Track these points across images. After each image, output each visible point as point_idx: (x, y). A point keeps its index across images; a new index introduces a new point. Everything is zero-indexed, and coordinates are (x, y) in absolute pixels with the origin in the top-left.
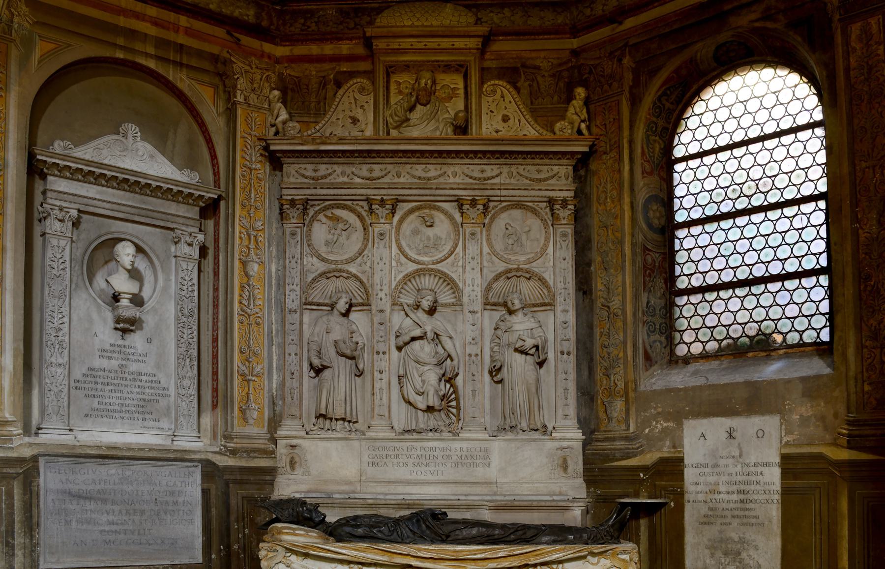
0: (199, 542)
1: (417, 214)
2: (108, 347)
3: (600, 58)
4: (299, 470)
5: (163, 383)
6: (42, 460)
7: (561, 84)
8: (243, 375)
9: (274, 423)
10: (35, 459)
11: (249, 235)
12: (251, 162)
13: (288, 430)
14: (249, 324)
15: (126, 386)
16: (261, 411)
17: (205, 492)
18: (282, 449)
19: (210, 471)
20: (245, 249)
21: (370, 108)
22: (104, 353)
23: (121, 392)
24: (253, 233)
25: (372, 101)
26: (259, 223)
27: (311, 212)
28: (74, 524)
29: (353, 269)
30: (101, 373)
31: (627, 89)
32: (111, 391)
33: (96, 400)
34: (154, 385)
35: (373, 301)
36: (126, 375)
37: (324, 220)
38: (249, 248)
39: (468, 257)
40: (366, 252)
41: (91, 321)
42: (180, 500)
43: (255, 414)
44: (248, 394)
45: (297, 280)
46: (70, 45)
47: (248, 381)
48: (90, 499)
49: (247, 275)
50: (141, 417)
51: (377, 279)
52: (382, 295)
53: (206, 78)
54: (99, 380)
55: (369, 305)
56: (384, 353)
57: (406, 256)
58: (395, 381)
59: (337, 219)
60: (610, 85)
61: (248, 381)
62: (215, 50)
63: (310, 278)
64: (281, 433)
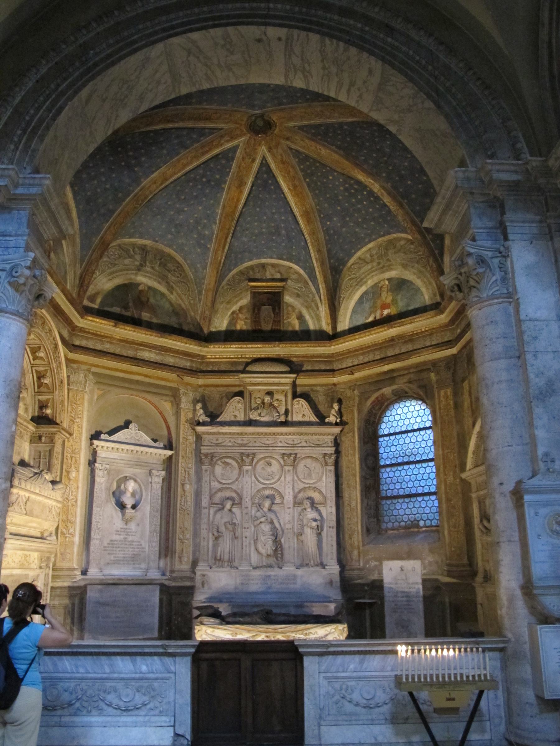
0: (156, 626)
1: (263, 461)
2: (119, 529)
3: (345, 388)
4: (206, 587)
5: (143, 546)
6: (89, 588)
7: (329, 399)
8: (180, 539)
9: (195, 563)
10: (85, 587)
11: (185, 471)
12: (187, 436)
13: (202, 567)
14: (184, 515)
15: (127, 548)
16: (188, 557)
17: (161, 600)
18: (198, 578)
19: (164, 589)
20: (183, 478)
21: (242, 410)
22: (118, 532)
23: (124, 551)
24: (187, 470)
25: (243, 408)
26: (190, 465)
27: (215, 460)
28: (100, 618)
29: (234, 487)
30: (116, 542)
31: (356, 405)
32: (119, 551)
33: (113, 556)
34: (139, 547)
35: (243, 503)
36: (127, 543)
37: (221, 464)
38: (185, 477)
39: (287, 482)
40: (240, 479)
41: (112, 518)
42: (149, 604)
43: (186, 559)
44: (182, 549)
45: (207, 493)
46: (109, 391)
47: (183, 543)
48: (108, 605)
49: (184, 490)
50: (132, 563)
51: (245, 492)
52: (247, 500)
53: (168, 399)
54: (115, 546)
55: (241, 505)
56: (248, 528)
57: (258, 481)
58: (252, 542)
59: (228, 464)
60: (350, 402)
61: (183, 543)
62: (172, 385)
63: (214, 491)
64: (198, 568)
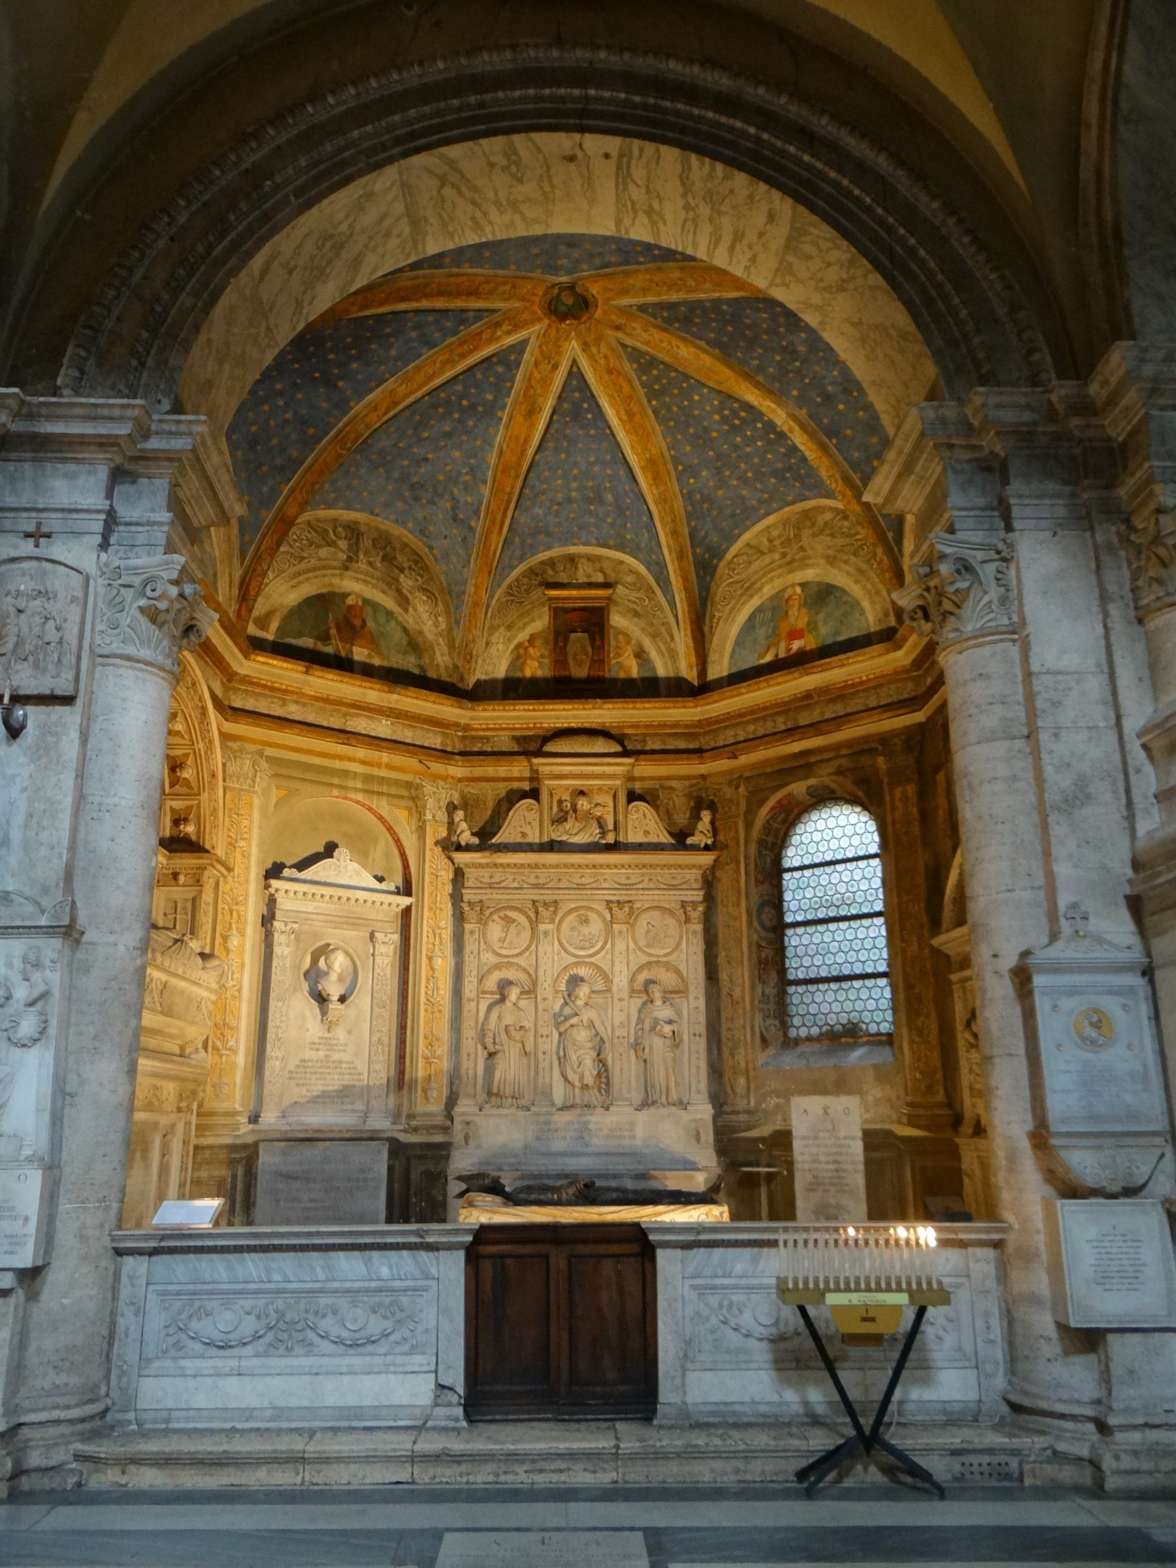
6: (262, 1146)
8: (426, 1058)
10: (256, 1145)
13: (465, 1107)
17: (390, 1169)
18: (458, 1126)
19: (397, 1149)
22: (314, 1046)
27: (487, 913)
29: (521, 961)
39: (616, 952)
43: (435, 1094)
49: (432, 969)
52: (546, 985)
57: (566, 951)
